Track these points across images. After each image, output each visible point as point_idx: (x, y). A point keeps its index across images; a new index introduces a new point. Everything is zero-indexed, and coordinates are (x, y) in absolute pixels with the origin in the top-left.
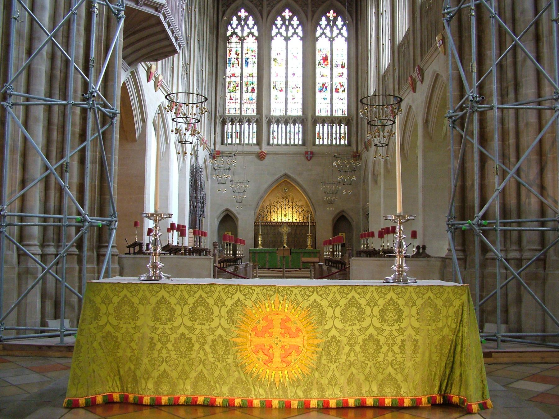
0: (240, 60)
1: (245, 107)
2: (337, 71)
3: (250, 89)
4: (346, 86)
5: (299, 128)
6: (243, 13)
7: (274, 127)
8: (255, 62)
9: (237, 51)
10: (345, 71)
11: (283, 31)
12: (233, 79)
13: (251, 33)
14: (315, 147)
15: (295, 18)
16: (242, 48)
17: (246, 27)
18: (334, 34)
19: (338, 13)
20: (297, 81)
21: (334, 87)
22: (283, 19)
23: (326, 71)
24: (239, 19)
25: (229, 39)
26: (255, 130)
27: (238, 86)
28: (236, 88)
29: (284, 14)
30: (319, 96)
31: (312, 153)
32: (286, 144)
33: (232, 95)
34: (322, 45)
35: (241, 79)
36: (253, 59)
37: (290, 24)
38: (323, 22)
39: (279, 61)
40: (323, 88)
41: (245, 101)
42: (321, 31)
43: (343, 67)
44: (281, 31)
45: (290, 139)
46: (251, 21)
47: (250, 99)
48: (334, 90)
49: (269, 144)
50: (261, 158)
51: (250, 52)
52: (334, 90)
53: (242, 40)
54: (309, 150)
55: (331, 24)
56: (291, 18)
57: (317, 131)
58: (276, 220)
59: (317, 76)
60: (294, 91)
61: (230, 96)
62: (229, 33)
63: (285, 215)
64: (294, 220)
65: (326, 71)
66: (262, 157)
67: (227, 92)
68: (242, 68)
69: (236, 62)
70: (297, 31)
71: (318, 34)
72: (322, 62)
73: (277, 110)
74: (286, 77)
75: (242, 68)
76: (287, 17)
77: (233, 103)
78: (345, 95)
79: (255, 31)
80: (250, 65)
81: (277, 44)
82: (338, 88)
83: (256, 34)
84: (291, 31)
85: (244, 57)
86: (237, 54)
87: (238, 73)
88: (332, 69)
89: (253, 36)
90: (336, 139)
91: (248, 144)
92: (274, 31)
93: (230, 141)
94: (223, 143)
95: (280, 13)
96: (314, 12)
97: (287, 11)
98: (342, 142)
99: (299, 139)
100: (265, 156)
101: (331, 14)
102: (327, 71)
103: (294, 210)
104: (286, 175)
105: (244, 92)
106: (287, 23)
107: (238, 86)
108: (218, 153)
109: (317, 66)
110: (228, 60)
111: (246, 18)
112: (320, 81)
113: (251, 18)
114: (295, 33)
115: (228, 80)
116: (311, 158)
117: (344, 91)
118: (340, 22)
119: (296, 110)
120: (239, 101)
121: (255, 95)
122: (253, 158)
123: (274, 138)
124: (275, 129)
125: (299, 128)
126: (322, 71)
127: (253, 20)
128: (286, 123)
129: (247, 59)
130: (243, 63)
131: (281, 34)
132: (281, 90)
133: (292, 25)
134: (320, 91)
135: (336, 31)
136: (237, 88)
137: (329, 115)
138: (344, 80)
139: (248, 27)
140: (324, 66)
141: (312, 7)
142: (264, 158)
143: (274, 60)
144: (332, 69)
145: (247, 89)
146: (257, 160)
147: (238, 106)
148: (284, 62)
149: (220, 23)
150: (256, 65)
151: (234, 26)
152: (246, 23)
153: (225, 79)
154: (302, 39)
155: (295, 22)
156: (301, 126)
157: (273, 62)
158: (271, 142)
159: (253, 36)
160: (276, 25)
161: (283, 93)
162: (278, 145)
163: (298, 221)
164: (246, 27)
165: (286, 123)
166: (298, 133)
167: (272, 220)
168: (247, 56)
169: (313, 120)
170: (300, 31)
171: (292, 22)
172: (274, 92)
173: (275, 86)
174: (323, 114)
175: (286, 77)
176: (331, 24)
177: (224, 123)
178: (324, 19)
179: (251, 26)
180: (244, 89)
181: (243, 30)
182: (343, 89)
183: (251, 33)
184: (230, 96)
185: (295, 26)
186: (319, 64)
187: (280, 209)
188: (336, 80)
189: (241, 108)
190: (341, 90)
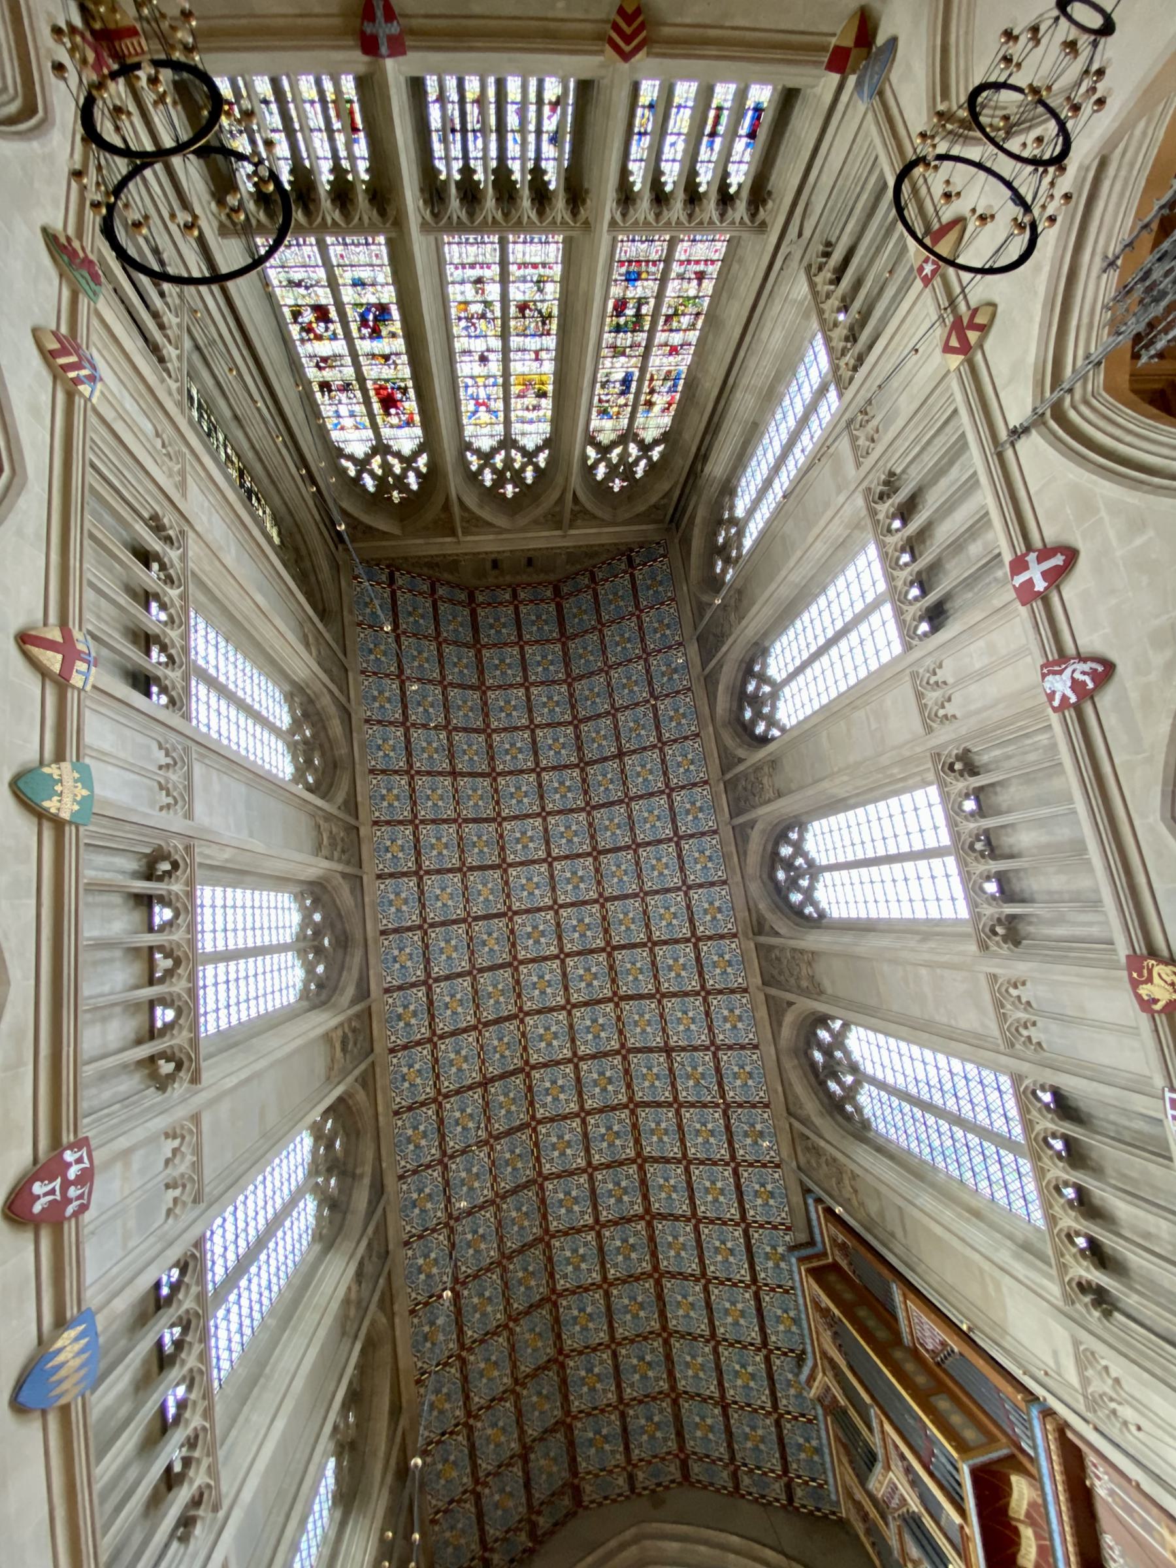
0: (646, 389)
3: (630, 312)
5: (447, 158)
8: (603, 385)
9: (648, 411)
11: (518, 459)
12: (676, 339)
18: (376, 462)
21: (337, 327)
23: (373, 371)
25: (665, 434)
27: (669, 318)
28: (676, 310)
35: (650, 340)
40: (376, 319)
41: (652, 269)
43: (325, 386)
47: (632, 278)
48: (333, 314)
50: (638, 11)
54: (390, 64)
57: (361, 148)
60: (476, 308)
61: (700, 284)
66: (629, 18)
67: (707, 300)
68: (643, 369)
75: (643, 369)
77: (697, 262)
80: (619, 375)
82: (322, 325)
86: (650, 404)
88: (361, 379)
100: (616, 27)
102: (373, 371)
105: (652, 301)
108: (839, 61)
109: (410, 384)
110: (680, 388)
115: (693, 336)
117: (296, 314)
120: (676, 268)
124: (548, 150)
125: (447, 158)
129: (623, 393)
132: (523, 307)
133: (495, 471)
134: (383, 309)
136: (671, 312)
140: (389, 385)
142: (621, 11)
143: (542, 394)
145: (639, 309)
148: (515, 390)
149: (682, 480)
151: (643, 463)
153: (701, 341)
156: (440, 165)
157: (549, 388)
161: (517, 293)
166: (448, 129)
168: (622, 401)
169: (391, 212)
173: (544, 323)
184: (700, 284)
186: (404, 391)
190: (308, 316)
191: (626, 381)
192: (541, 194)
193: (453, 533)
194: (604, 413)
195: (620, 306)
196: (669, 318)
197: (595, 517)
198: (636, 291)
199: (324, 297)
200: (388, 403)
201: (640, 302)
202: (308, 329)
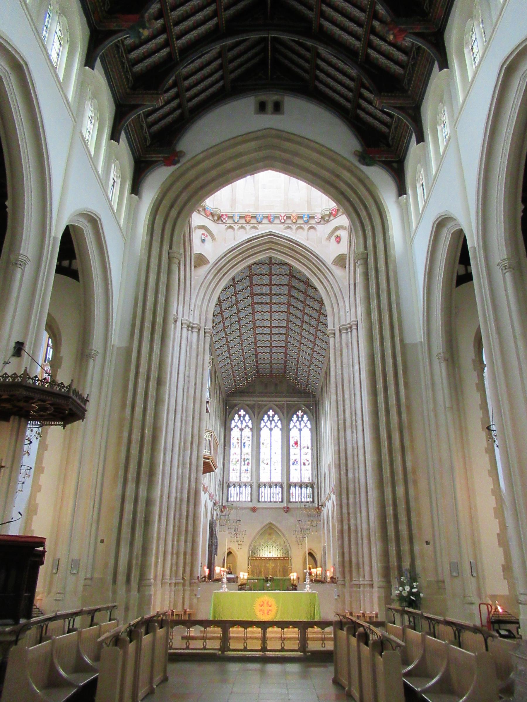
0: (240, 443)
1: (243, 475)
2: (304, 451)
3: (246, 462)
4: (310, 461)
6: (242, 413)
7: (262, 489)
10: (309, 451)
12: (235, 456)
13: (247, 426)
14: (290, 504)
15: (276, 416)
16: (241, 435)
17: (244, 421)
18: (302, 426)
20: (277, 457)
22: (269, 416)
23: (297, 450)
24: (240, 416)
26: (250, 491)
29: (269, 413)
30: (292, 467)
31: (288, 508)
33: (235, 467)
34: (294, 433)
36: (249, 443)
37: (273, 420)
38: (295, 418)
39: (265, 444)
42: (293, 424)
43: (308, 448)
44: (267, 424)
45: (273, 497)
47: (247, 470)
48: (302, 464)
49: (259, 501)
51: (246, 438)
52: (302, 464)
53: (242, 430)
54: (285, 506)
56: (273, 416)
58: (264, 556)
59: (291, 454)
62: (232, 426)
63: (270, 552)
64: (276, 556)
65: (297, 450)
68: (241, 449)
69: (237, 445)
70: (277, 424)
71: (291, 426)
72: (294, 445)
73: (263, 478)
74: (271, 455)
75: (241, 449)
76: (271, 415)
78: (309, 467)
79: (250, 424)
81: (265, 433)
83: (251, 426)
85: (243, 442)
86: (238, 440)
88: (301, 449)
89: (249, 427)
90: (304, 497)
91: (245, 502)
93: (232, 500)
94: (227, 501)
95: (266, 413)
96: (288, 413)
97: (271, 411)
98: (308, 500)
99: (279, 498)
101: (300, 413)
103: (277, 548)
104: (270, 523)
106: (271, 419)
107: (238, 461)
108: (224, 507)
111: (244, 416)
112: (292, 458)
113: (247, 416)
114: (276, 426)
115: (232, 457)
116: (287, 511)
117: (309, 464)
118: (305, 418)
119: (277, 478)
121: (250, 467)
123: (262, 497)
126: (294, 451)
127: (249, 417)
128: (270, 487)
131: (267, 426)
132: (267, 464)
133: (274, 421)
134: (293, 464)
137: (299, 481)
138: (309, 457)
139: (245, 422)
141: (287, 410)
143: (263, 443)
144: (301, 449)
147: (238, 475)
150: (250, 447)
152: (244, 419)
154: (281, 429)
155: (276, 418)
157: (261, 445)
158: (260, 500)
159: (249, 427)
160: (264, 420)
162: (265, 502)
163: (279, 556)
164: (244, 421)
165: (270, 487)
166: (278, 494)
167: (261, 556)
170: (279, 424)
171: (274, 418)
172: (262, 465)
175: (271, 455)
176: (300, 419)
177: (229, 486)
178: (295, 416)
179: (247, 421)
180: (243, 463)
182: (308, 463)
183: (247, 426)
185: (276, 421)
186: (293, 446)
187: (266, 548)
188: (304, 457)
189: (240, 476)
191: (245, 446)
193: (287, 404)
194: (248, 438)
195: (248, 464)
196: (238, 461)
197: (248, 406)
201: (244, 464)
202: (308, 461)
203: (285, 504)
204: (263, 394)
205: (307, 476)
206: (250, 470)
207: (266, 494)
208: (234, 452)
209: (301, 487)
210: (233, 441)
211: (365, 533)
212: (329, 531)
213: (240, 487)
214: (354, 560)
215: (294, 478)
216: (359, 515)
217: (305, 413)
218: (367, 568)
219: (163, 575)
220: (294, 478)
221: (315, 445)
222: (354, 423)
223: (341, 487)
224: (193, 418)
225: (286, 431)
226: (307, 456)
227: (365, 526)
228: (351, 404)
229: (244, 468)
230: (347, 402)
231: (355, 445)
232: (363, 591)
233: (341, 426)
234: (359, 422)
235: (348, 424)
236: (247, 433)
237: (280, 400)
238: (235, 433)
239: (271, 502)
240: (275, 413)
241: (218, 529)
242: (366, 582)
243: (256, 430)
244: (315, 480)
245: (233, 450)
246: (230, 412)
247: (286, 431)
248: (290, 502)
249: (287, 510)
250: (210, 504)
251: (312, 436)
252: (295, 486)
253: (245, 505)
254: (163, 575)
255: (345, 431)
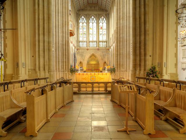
1: (84, 38)
3: (85, 34)
11: (92, 21)
12: (81, 32)
15: (95, 18)
19: (104, 17)
20: (95, 33)
22: (92, 18)
23: (102, 30)
24: (82, 18)
32: (93, 47)
34: (101, 24)
38: (101, 19)
46: (85, 19)
49: (89, 47)
53: (83, 23)
55: (103, 20)
56: (94, 18)
71: (100, 22)
79: (86, 21)
81: (91, 24)
83: (86, 22)
84: (94, 21)
85: (84, 27)
87: (82, 31)
92: (90, 21)
96: (99, 17)
99: (96, 46)
101: (103, 17)
111: (84, 18)
112: (100, 33)
113: (85, 18)
115: (80, 32)
118: (104, 19)
122: (86, 50)
128: (93, 42)
130: (83, 29)
135: (104, 21)
138: (106, 32)
146: (87, 51)
147: (82, 38)
155: (95, 19)
157: (90, 29)
162: (91, 47)
165: (93, 42)
170: (96, 21)
172: (90, 35)
174: (101, 40)
176: (103, 20)
177: (79, 42)
181: (83, 21)
190: (105, 35)
192: (91, 42)
198: (85, 36)
199: (103, 36)
200: (101, 28)
203: (98, 48)
204: (90, 10)
205: (105, 38)
206: (86, 37)
207: (91, 44)
208: (81, 31)
209: (103, 42)
210: (80, 27)
211: (125, 55)
212: (112, 55)
213: (83, 42)
214: (121, 63)
215: (101, 39)
216: (123, 49)
217: (105, 17)
218: (125, 66)
219: (59, 69)
220: (101, 39)
221: (107, 28)
222: (123, 17)
223: (117, 40)
224: (65, 15)
225: (98, 24)
226: (105, 32)
227: (125, 52)
228: (122, 10)
229: (84, 36)
230: (121, 9)
231: (123, 25)
232: (124, 73)
233: (119, 18)
234: (125, 17)
235: (121, 17)
236: (85, 24)
237: (96, 13)
238: (81, 24)
239: (93, 47)
240: (94, 17)
241: (76, 56)
242: (125, 70)
243: (88, 23)
244: (107, 40)
245: (80, 30)
246: (79, 17)
247: (98, 24)
248: (99, 47)
249: (98, 49)
250: (73, 48)
251: (106, 25)
252: (101, 42)
253: (85, 48)
254: (59, 69)
255: (120, 20)
